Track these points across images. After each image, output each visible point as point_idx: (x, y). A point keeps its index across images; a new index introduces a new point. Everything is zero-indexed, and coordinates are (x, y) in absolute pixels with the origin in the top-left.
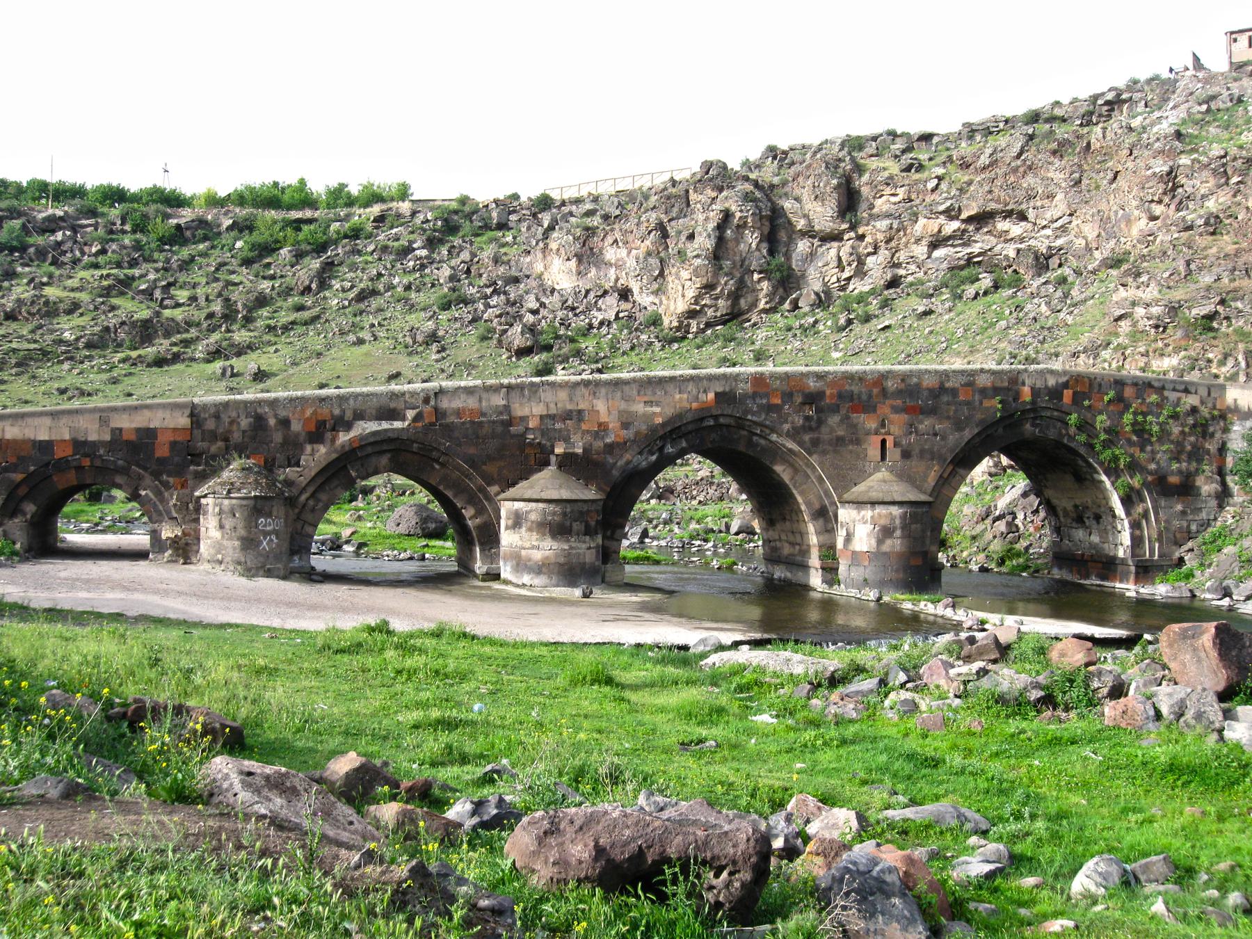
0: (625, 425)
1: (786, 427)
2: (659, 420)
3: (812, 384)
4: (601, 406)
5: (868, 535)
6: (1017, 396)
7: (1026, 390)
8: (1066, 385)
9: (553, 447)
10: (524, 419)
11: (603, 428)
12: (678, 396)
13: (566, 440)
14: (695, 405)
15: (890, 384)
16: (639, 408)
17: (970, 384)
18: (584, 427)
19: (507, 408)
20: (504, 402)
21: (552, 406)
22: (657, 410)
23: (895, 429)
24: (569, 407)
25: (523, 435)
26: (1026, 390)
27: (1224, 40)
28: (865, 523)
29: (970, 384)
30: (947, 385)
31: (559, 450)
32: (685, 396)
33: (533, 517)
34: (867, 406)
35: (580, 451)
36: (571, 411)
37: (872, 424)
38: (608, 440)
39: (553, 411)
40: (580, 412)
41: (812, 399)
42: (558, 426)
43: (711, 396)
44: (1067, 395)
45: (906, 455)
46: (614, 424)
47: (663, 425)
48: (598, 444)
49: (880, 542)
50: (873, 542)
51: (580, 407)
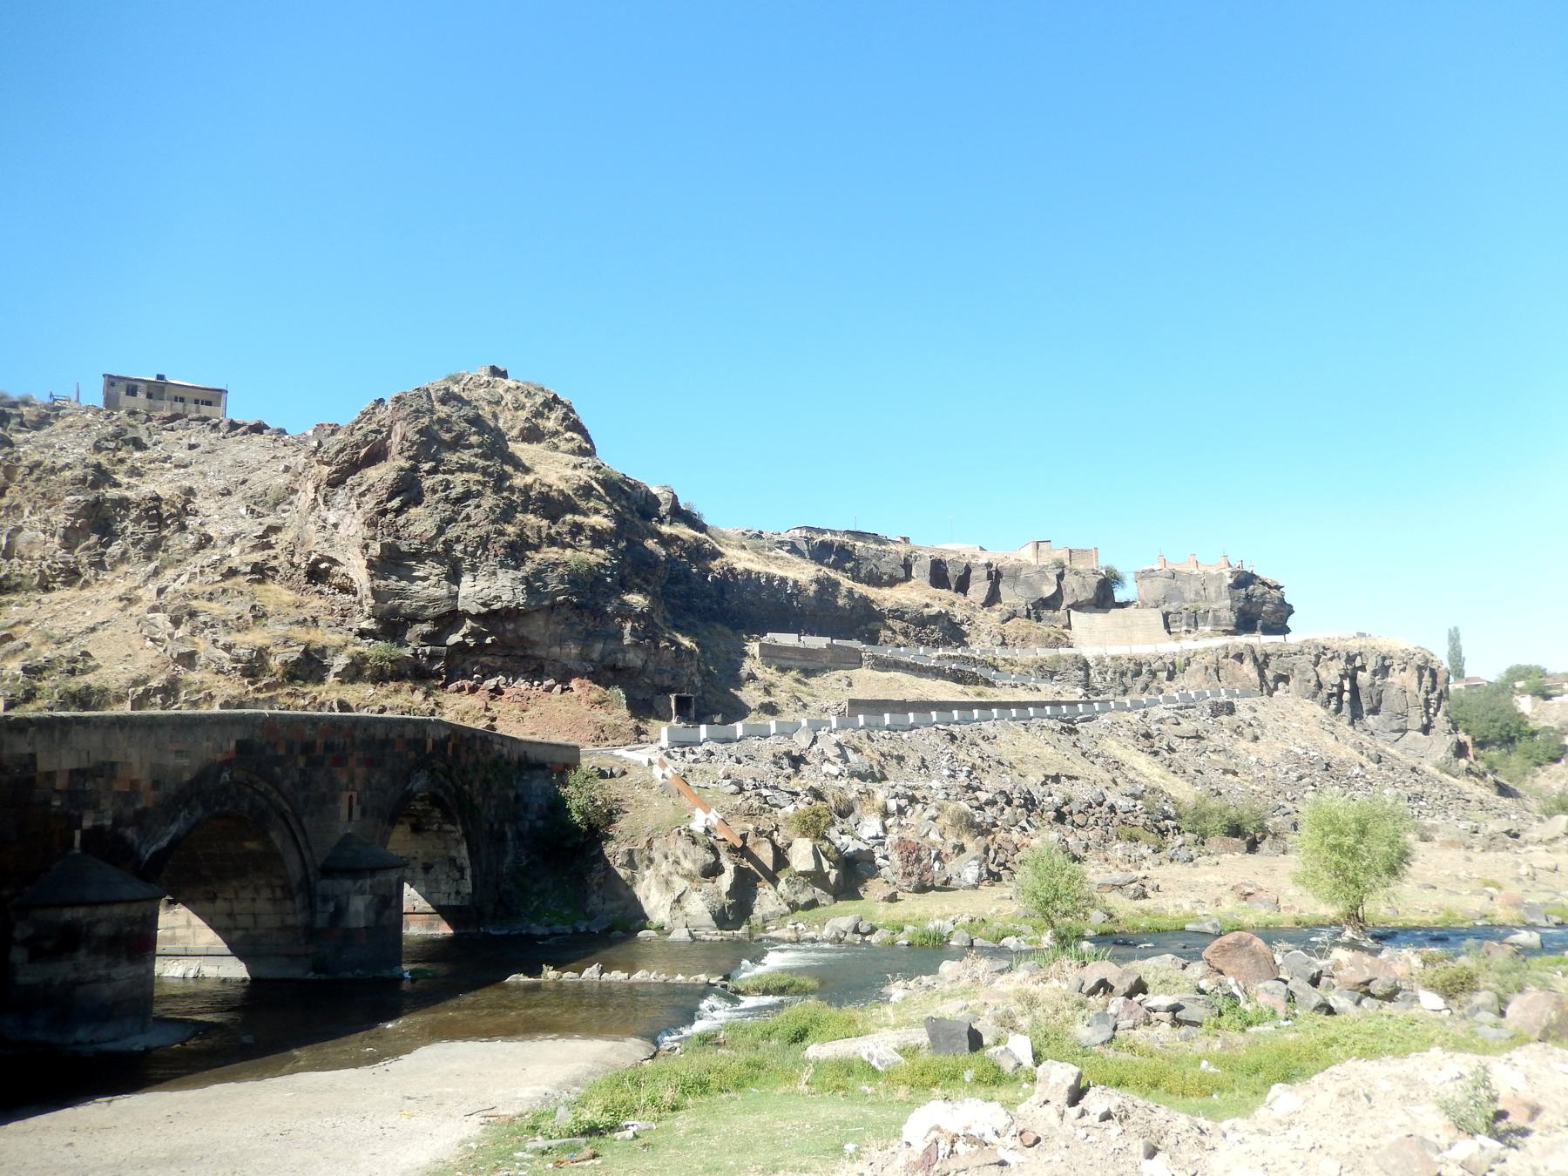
0: (156, 784)
1: (287, 783)
2: (187, 777)
3: (309, 732)
4: (134, 756)
5: (367, 907)
6: (425, 747)
7: (430, 741)
8: (448, 738)
9: (80, 818)
10: (50, 776)
11: (134, 784)
12: (205, 744)
13: (95, 806)
14: (220, 757)
15: (358, 734)
16: (171, 761)
17: (401, 736)
18: (117, 787)
19: (33, 756)
20: (29, 750)
21: (84, 755)
22: (185, 762)
23: (358, 784)
24: (102, 758)
25: (47, 802)
26: (430, 741)
27: (100, 384)
28: (363, 893)
29: (401, 736)
30: (391, 735)
31: (87, 823)
32: (211, 744)
33: (103, 930)
34: (340, 761)
35: (108, 823)
36: (104, 764)
37: (344, 780)
38: (139, 806)
39: (84, 765)
40: (113, 765)
41: (308, 748)
42: (89, 786)
43: (233, 744)
44: (450, 745)
45: (364, 813)
46: (145, 783)
47: (191, 783)
48: (129, 812)
49: (379, 914)
50: (372, 915)
51: (113, 759)
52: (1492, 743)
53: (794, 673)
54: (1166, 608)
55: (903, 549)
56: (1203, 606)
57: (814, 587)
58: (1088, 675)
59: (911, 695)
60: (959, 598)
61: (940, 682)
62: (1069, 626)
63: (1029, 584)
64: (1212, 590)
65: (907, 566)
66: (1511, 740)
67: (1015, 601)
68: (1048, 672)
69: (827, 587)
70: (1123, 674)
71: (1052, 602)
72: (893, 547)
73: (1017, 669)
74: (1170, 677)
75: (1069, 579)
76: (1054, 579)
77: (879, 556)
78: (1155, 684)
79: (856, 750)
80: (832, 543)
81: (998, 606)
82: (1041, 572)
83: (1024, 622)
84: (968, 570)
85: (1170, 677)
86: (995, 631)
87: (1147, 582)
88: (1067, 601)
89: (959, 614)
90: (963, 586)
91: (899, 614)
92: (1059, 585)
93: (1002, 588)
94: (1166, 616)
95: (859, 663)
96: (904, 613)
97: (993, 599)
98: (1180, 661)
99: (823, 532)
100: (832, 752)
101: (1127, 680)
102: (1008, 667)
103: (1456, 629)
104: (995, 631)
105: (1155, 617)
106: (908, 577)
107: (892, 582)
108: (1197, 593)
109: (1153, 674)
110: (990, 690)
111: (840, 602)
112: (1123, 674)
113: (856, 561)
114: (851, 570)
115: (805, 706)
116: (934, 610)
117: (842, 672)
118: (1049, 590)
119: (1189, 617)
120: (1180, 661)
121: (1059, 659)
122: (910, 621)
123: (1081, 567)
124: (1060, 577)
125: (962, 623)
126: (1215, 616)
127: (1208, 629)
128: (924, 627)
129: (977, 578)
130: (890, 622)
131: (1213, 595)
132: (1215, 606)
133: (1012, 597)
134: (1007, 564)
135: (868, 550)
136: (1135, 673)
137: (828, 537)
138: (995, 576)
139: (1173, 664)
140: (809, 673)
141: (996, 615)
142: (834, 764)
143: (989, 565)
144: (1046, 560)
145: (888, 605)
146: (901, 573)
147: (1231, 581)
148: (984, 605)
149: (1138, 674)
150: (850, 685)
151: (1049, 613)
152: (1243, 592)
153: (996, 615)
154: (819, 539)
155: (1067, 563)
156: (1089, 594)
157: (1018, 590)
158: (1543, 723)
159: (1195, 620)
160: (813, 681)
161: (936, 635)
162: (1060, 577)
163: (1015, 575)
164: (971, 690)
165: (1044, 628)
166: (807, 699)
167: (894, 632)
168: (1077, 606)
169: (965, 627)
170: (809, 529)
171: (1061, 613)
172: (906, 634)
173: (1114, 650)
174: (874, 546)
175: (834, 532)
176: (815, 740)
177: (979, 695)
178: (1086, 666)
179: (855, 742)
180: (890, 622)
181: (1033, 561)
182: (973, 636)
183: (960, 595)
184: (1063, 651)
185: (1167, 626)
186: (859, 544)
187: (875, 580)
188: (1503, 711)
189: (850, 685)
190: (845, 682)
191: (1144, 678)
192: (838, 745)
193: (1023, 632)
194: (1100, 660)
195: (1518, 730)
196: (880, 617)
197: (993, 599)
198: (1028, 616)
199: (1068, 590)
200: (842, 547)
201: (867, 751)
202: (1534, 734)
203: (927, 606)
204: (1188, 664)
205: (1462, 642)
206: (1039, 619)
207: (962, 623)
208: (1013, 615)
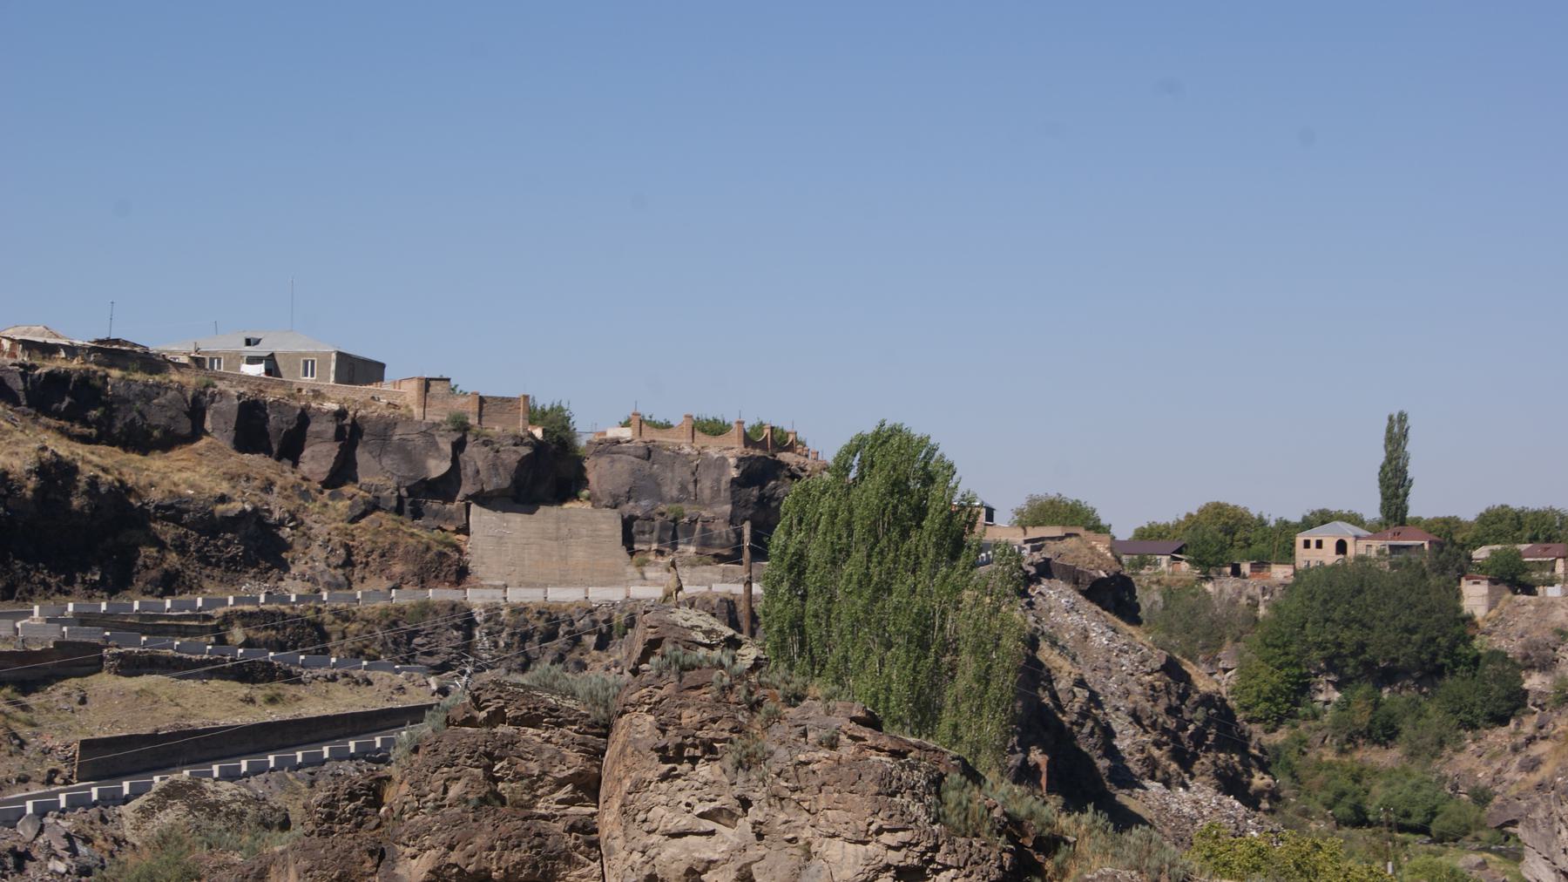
52: (1406, 673)
53: (7, 691)
54: (629, 508)
55: (191, 380)
56: (689, 510)
57: (32, 483)
58: (469, 636)
59: (163, 720)
60: (285, 475)
61: (215, 683)
62: (465, 530)
63: (404, 451)
64: (706, 484)
65: (196, 410)
66: (1439, 672)
67: (377, 480)
68: (402, 640)
69: (56, 473)
70: (526, 637)
71: (444, 488)
72: (175, 377)
73: (354, 627)
74: (602, 645)
75: (475, 455)
76: (448, 449)
77: (148, 394)
78: (575, 655)
79: (87, 840)
80: (68, 374)
81: (348, 489)
82: (429, 432)
83: (386, 520)
84: (304, 418)
85: (602, 645)
86: (336, 539)
87: (604, 462)
88: (467, 488)
89: (278, 507)
90: (291, 449)
91: (173, 511)
92: (455, 460)
93: (362, 457)
94: (627, 523)
95: (96, 667)
96: (182, 512)
97: (342, 473)
98: (619, 618)
99: (49, 350)
100: (59, 845)
101: (532, 647)
102: (339, 625)
103: (1402, 418)
104: (336, 539)
105: (610, 524)
106: (197, 432)
107: (169, 441)
108: (683, 488)
109: (576, 640)
110: (292, 690)
111: (76, 503)
112: (526, 637)
113: (108, 405)
114: (97, 422)
115: (22, 744)
116: (235, 507)
117: (74, 681)
118: (437, 467)
119: (664, 528)
120: (619, 618)
121: (425, 609)
122: (190, 526)
123: (495, 429)
124: (459, 446)
125: (281, 523)
126: (704, 530)
127: (692, 549)
128: (215, 536)
129: (318, 435)
130: (157, 526)
131: (707, 493)
132: (706, 514)
133: (377, 473)
134: (372, 412)
135: (129, 383)
136: (549, 633)
137: (59, 363)
138: (350, 432)
139: (608, 621)
140: (27, 686)
141: (342, 505)
142: (61, 859)
143: (341, 414)
144: (437, 414)
145: (156, 495)
146: (185, 427)
147: (735, 473)
148: (326, 484)
149: (551, 635)
150: (83, 701)
151: (435, 505)
152: (755, 492)
153: (342, 505)
154: (46, 367)
155: (473, 420)
156: (502, 481)
157: (387, 462)
158: (1500, 643)
159: (673, 533)
160: (33, 700)
161: (232, 550)
162: (459, 446)
163: (384, 430)
164: (261, 691)
165: (419, 533)
166: (25, 732)
167: (162, 546)
168: (484, 499)
169: (286, 532)
170: (28, 345)
171: (455, 506)
172: (181, 548)
173: (516, 596)
174: (139, 376)
175: (72, 351)
176: (41, 830)
177: (272, 700)
178: (469, 624)
179: (87, 830)
180: (157, 526)
181: (417, 412)
182: (298, 547)
183: (286, 465)
184: (437, 594)
185: (628, 540)
186: (115, 373)
187: (140, 441)
188: (1429, 612)
189: (83, 701)
190: (76, 696)
191: (560, 643)
192: (68, 836)
193: (385, 541)
194: (492, 612)
195: (1451, 651)
196: (141, 518)
197: (342, 473)
198: (399, 510)
199: (469, 471)
200: (85, 380)
201: (99, 841)
202: (1477, 660)
203: (223, 499)
204: (631, 623)
205: (1410, 447)
206: (417, 514)
207: (281, 523)
208: (373, 506)
